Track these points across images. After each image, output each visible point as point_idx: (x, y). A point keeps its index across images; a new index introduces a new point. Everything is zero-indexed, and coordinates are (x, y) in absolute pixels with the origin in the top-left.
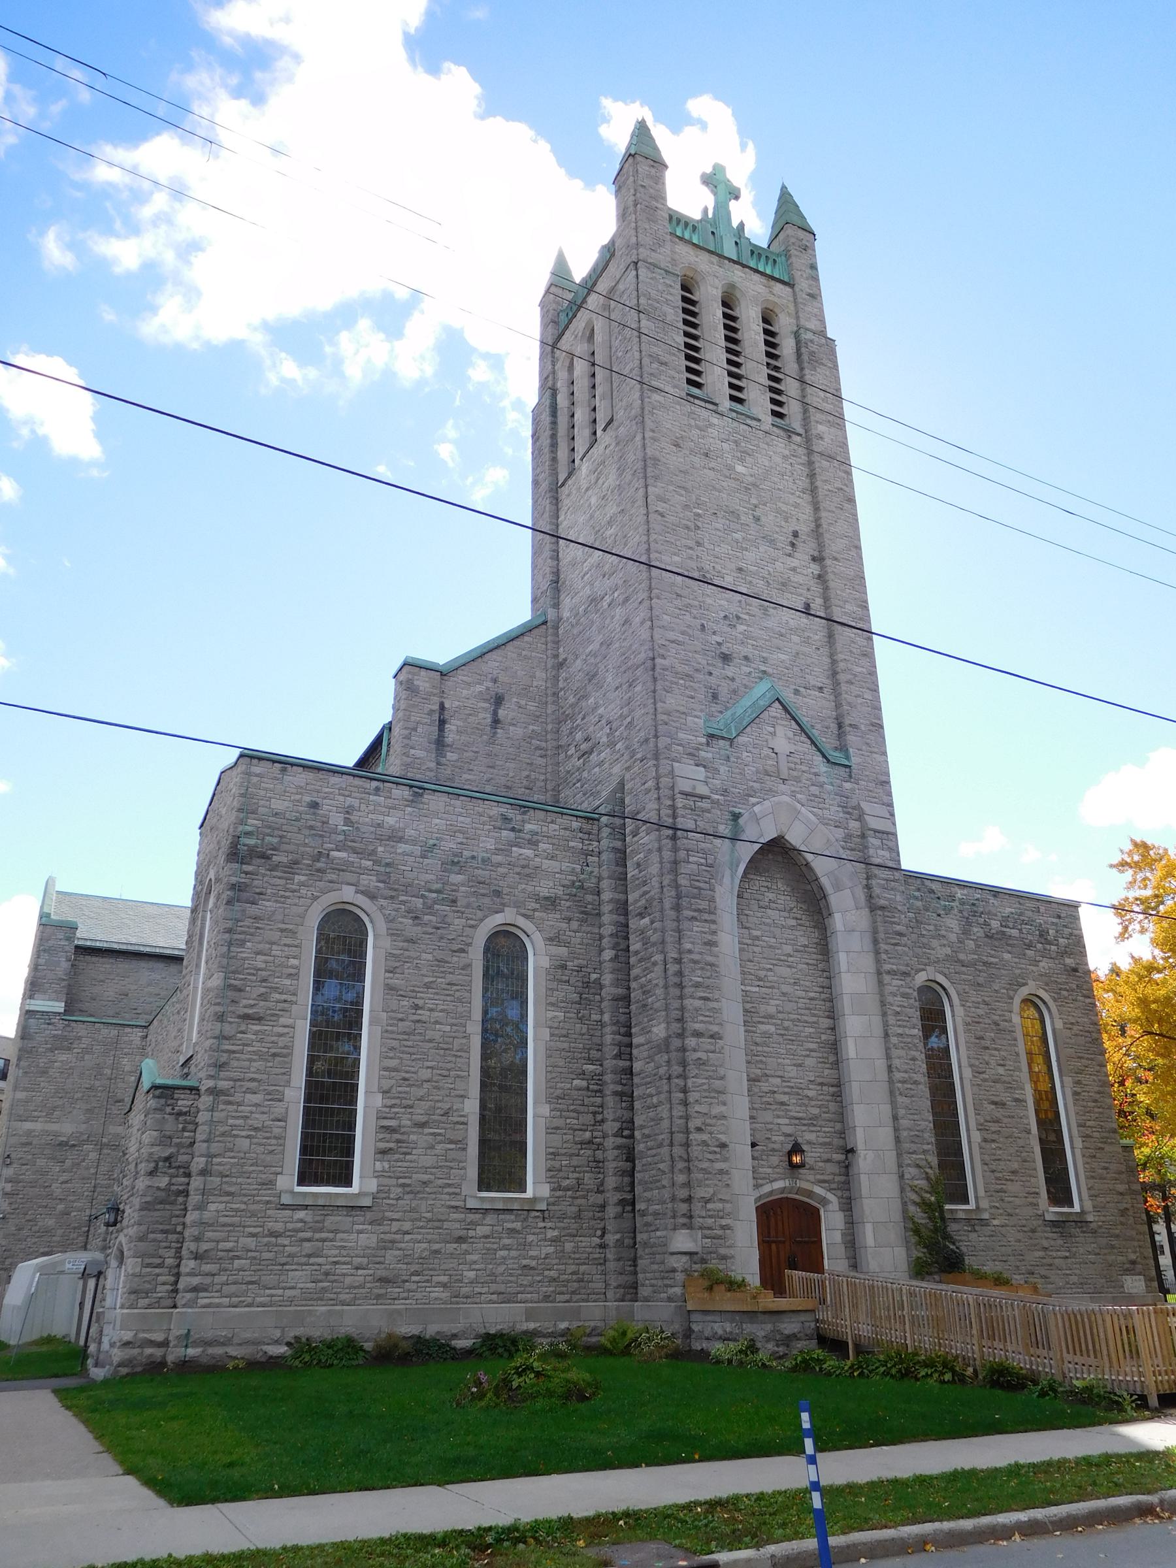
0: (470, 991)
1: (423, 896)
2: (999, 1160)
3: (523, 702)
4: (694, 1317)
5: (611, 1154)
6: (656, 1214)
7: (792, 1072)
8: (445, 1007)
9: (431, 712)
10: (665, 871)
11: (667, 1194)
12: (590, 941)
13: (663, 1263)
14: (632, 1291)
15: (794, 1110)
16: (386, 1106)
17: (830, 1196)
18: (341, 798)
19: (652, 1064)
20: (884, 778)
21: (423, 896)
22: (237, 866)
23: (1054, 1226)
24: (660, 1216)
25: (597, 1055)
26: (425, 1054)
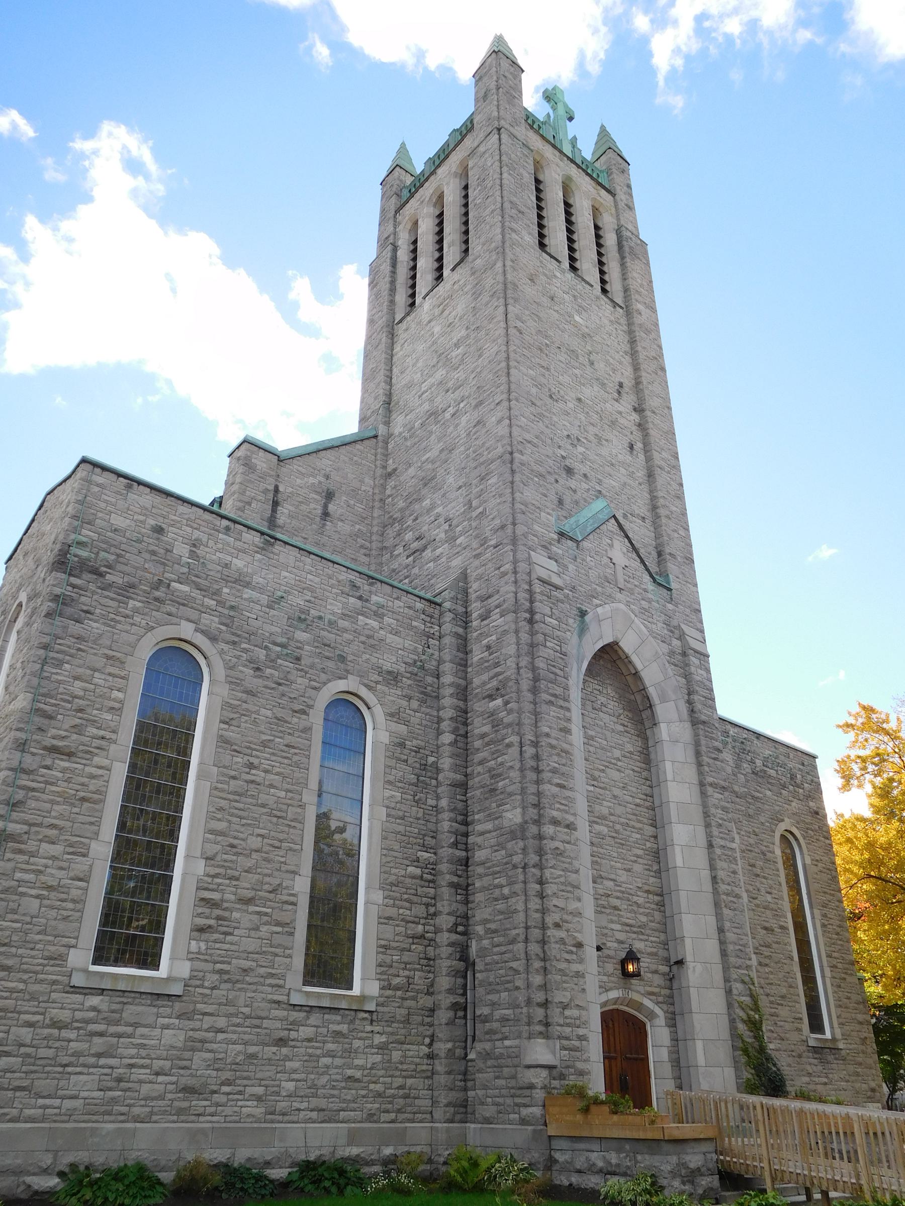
0: (308, 757)
1: (266, 648)
2: (771, 984)
3: (352, 502)
4: (556, 1144)
5: (445, 951)
6: (504, 1020)
7: (623, 877)
8: (283, 770)
9: (266, 491)
10: (523, 652)
11: (521, 998)
12: (429, 724)
13: (514, 1077)
14: (462, 1110)
15: (627, 917)
16: (208, 875)
17: (657, 1010)
18: (189, 529)
19: (503, 852)
20: (697, 607)
21: (266, 648)
22: (63, 576)
23: (815, 1052)
24: (511, 1023)
25: (429, 841)
26: (255, 819)
